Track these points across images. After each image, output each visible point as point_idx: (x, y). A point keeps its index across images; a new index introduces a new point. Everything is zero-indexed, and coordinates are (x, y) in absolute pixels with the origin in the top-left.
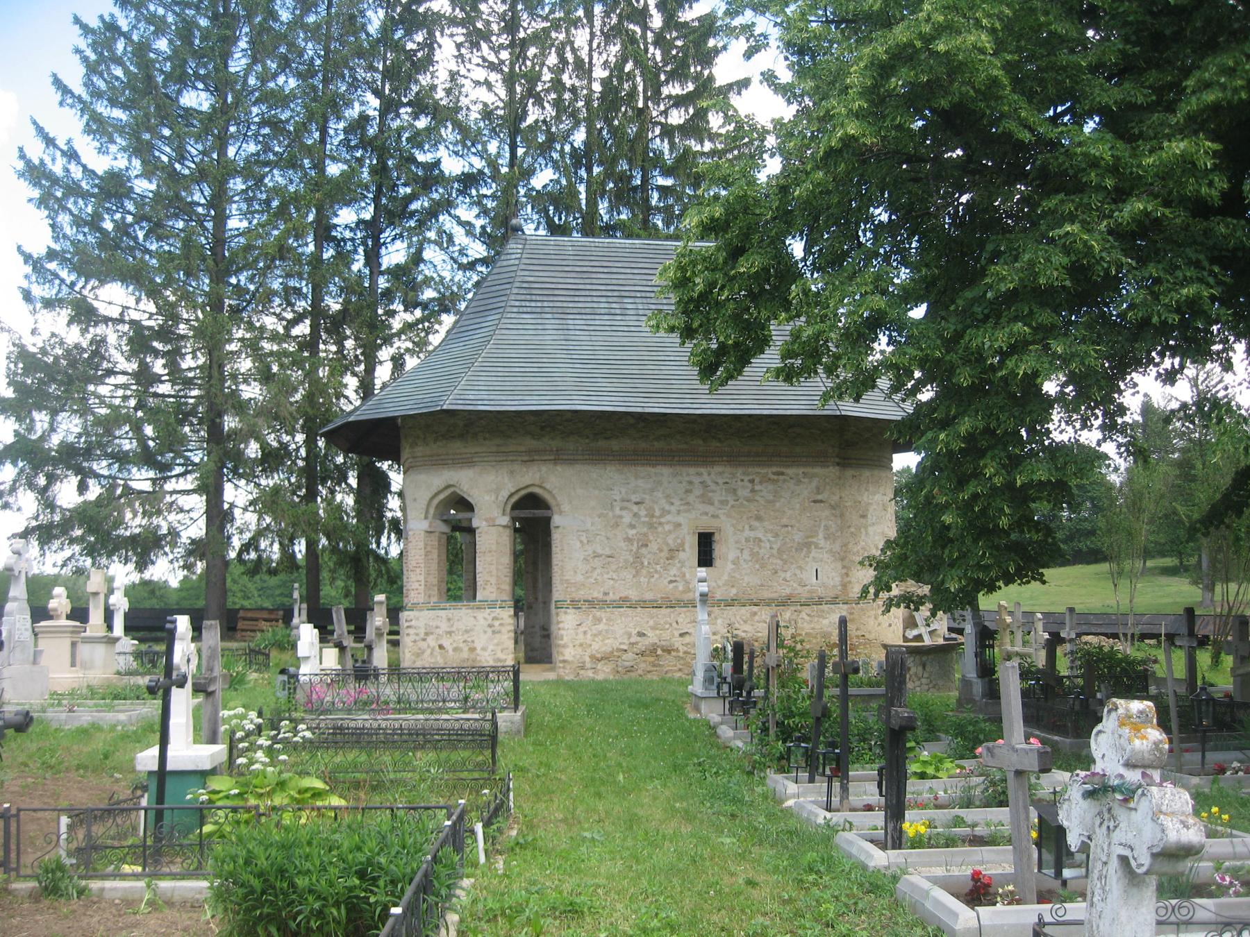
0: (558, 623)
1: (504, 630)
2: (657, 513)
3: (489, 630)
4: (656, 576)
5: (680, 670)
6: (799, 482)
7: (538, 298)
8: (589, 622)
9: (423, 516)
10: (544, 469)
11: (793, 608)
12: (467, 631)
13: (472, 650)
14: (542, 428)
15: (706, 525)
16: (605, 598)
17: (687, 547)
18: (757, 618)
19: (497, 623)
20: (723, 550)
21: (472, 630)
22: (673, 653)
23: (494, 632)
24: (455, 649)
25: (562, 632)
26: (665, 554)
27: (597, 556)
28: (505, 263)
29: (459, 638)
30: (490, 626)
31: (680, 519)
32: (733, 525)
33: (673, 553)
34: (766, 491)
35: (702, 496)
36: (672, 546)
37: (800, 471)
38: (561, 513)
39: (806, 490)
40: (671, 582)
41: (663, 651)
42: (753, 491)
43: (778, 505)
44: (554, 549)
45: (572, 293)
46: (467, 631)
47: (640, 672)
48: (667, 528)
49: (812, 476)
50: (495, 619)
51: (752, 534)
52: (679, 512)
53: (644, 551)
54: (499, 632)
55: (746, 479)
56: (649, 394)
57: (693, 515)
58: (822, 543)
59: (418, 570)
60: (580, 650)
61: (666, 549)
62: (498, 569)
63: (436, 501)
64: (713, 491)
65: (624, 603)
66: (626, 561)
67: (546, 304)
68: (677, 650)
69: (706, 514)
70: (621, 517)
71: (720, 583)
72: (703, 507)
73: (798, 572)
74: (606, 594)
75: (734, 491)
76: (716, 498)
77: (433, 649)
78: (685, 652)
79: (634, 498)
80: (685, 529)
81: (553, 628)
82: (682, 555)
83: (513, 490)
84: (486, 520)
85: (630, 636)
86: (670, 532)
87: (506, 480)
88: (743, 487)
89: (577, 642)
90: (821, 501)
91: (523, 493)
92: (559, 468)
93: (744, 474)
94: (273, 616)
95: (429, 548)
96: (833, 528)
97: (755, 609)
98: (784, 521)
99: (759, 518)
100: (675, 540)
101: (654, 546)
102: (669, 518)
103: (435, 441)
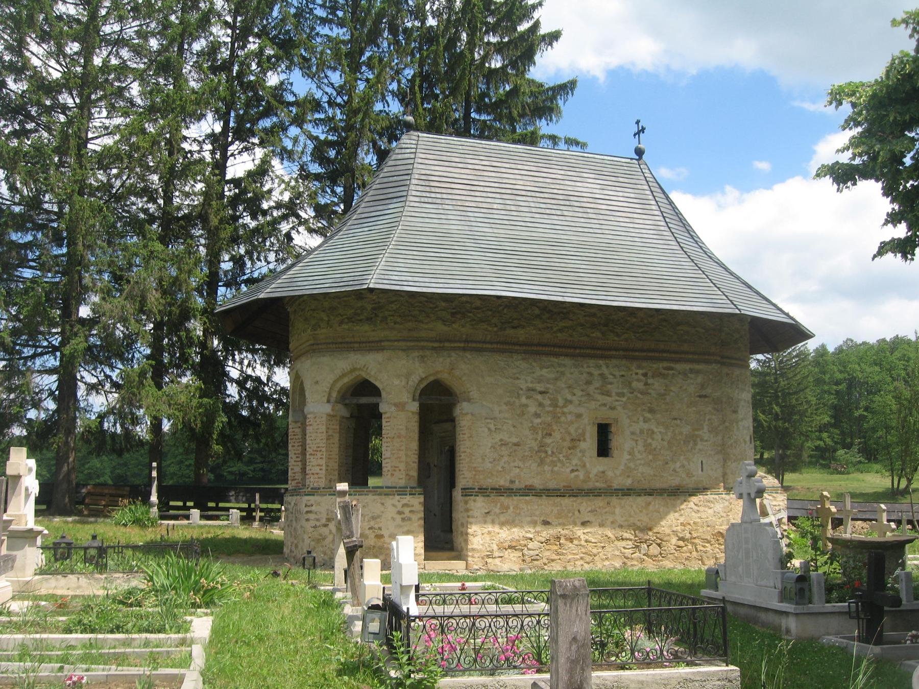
1: (414, 517)
2: (561, 402)
3: (398, 518)
4: (559, 465)
5: (582, 558)
7: (437, 190)
8: (497, 511)
9: (325, 399)
12: (374, 518)
15: (604, 416)
16: (511, 486)
17: (588, 435)
18: (651, 507)
19: (406, 510)
20: (620, 442)
21: (379, 517)
22: (575, 542)
23: (403, 519)
26: (567, 444)
30: (400, 513)
31: (581, 410)
32: (628, 417)
33: (575, 441)
34: (657, 384)
36: (574, 435)
37: (687, 366)
41: (566, 539)
42: (646, 384)
43: (668, 397)
45: (468, 187)
46: (374, 518)
47: (545, 561)
48: (569, 417)
49: (698, 372)
50: (404, 506)
51: (646, 426)
53: (548, 440)
54: (410, 519)
55: (640, 372)
56: (563, 284)
57: (593, 405)
59: (319, 454)
61: (568, 438)
62: (407, 455)
63: (339, 385)
64: (611, 383)
65: (529, 491)
69: (605, 405)
70: (526, 406)
71: (618, 472)
73: (685, 463)
74: (512, 482)
76: (614, 389)
79: (539, 387)
82: (583, 445)
84: (396, 405)
86: (572, 422)
87: (417, 364)
88: (638, 380)
90: (705, 396)
91: (432, 379)
92: (468, 355)
93: (639, 367)
94: (120, 492)
95: (330, 432)
97: (649, 498)
99: (651, 411)
100: (576, 430)
101: (557, 435)
102: (570, 408)
103: (341, 323)
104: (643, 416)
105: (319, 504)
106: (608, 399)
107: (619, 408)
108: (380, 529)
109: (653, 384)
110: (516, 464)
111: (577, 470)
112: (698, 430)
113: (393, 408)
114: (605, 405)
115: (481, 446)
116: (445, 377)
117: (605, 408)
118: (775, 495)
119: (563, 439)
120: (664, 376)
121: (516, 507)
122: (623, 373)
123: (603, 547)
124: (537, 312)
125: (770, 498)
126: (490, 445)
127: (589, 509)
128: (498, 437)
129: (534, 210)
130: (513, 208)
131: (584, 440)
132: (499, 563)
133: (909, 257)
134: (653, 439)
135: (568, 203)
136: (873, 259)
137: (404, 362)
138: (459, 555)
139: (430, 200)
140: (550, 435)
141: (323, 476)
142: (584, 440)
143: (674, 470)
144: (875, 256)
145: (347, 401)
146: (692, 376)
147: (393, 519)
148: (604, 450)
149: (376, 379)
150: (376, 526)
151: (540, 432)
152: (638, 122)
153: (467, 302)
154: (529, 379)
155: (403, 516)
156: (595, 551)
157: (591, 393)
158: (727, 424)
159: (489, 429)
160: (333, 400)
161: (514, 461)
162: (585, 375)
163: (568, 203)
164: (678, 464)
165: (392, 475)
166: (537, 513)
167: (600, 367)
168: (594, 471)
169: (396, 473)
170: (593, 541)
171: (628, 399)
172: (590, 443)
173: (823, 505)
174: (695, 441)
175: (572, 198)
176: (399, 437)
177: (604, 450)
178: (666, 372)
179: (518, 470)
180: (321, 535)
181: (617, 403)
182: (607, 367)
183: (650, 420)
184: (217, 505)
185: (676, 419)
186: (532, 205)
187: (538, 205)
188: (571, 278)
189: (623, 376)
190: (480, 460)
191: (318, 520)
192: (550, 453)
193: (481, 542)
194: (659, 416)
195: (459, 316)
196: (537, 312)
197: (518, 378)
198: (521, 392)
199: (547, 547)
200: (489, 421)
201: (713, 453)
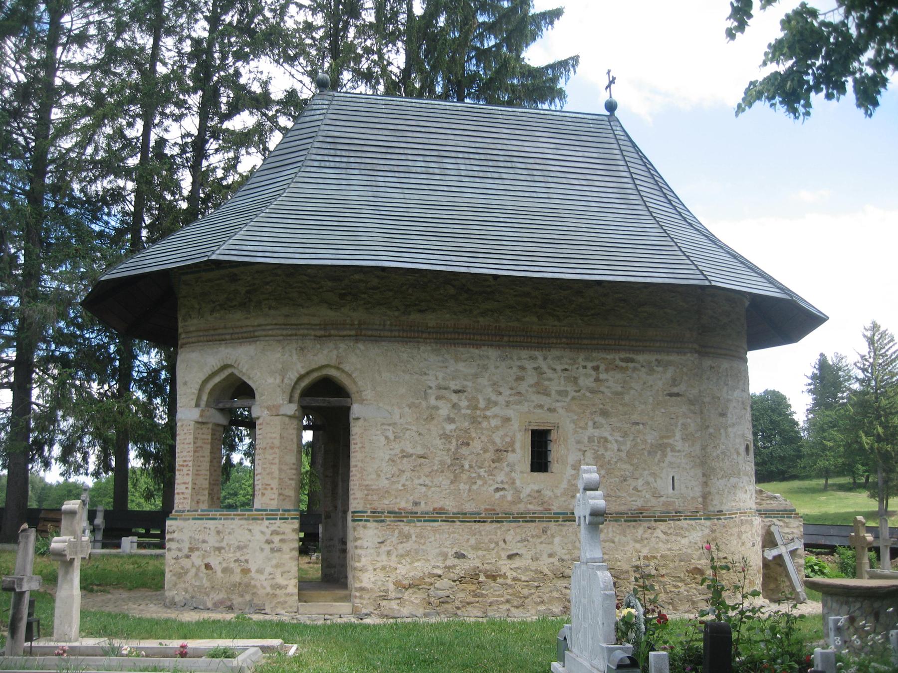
0: (356, 539)
1: (286, 547)
2: (482, 404)
4: (479, 482)
5: (508, 601)
6: (651, 371)
7: (344, 153)
8: (394, 540)
9: (193, 403)
10: (342, 346)
11: (646, 524)
12: (240, 548)
13: (246, 571)
14: (342, 296)
15: (541, 420)
16: (415, 509)
17: (518, 445)
19: (276, 539)
21: (246, 547)
22: (499, 580)
23: (272, 550)
24: (225, 570)
25: (359, 551)
26: (490, 455)
27: (406, 455)
28: (308, 119)
29: (230, 556)
30: (268, 542)
31: (510, 413)
32: (573, 421)
33: (500, 453)
34: (612, 381)
35: (537, 384)
37: (652, 357)
38: (362, 401)
39: (660, 380)
40: (497, 490)
41: (487, 577)
42: (597, 380)
43: (627, 398)
44: (352, 447)
46: (240, 548)
47: (457, 603)
48: (494, 422)
50: (274, 533)
51: (597, 433)
52: (508, 404)
53: (464, 451)
54: (279, 550)
55: (590, 365)
56: (474, 254)
57: (525, 408)
58: (679, 445)
59: (185, 469)
60: (381, 575)
61: (492, 449)
62: (280, 470)
63: (210, 385)
64: (550, 380)
65: (439, 515)
66: (442, 463)
67: (352, 160)
68: (504, 576)
69: (541, 406)
70: (437, 408)
71: (558, 492)
72: (537, 399)
73: (651, 479)
74: (416, 504)
75: (576, 379)
76: (554, 387)
77: (198, 569)
78: (514, 579)
79: (453, 385)
80: (515, 425)
81: (350, 545)
82: (511, 457)
83: (303, 372)
84: (268, 408)
85: (445, 556)
86: (497, 428)
87: (295, 357)
89: (379, 565)
90: (678, 395)
91: (315, 375)
92: (361, 346)
93: (587, 359)
95: (199, 443)
96: (692, 427)
98: (635, 417)
99: (604, 413)
101: (477, 446)
102: (495, 410)
103: (212, 312)
104: (592, 419)
105: (181, 530)
106: (545, 401)
107: (560, 411)
108: (247, 561)
109: (607, 380)
110: (421, 481)
111: (503, 489)
112: (668, 437)
113: (266, 412)
115: (376, 460)
116: (333, 372)
117: (540, 411)
118: (787, 520)
121: (420, 536)
122: (567, 367)
123: (537, 587)
124: (452, 291)
125: (781, 523)
126: (387, 457)
127: (518, 538)
128: (397, 447)
129: (463, 173)
130: (437, 171)
131: (513, 451)
132: (396, 607)
133: (801, 110)
134: (606, 449)
135: (509, 165)
136: (737, 115)
137: (279, 355)
138: (302, 598)
139: (332, 165)
140: (468, 444)
141: (189, 496)
142: (513, 451)
143: (635, 489)
144: (740, 109)
145: (221, 406)
146: (660, 369)
147: (262, 550)
148: (540, 461)
149: (249, 378)
150: (242, 558)
151: (454, 441)
152: (609, 72)
153: (360, 281)
154: (440, 375)
155: (272, 546)
156: (526, 592)
157: (523, 392)
158: (711, 430)
159: (387, 438)
160: (203, 403)
161: (419, 478)
162: (515, 369)
163: (509, 165)
165: (263, 494)
166: (447, 543)
168: (527, 491)
169: (268, 492)
170: (524, 578)
172: (522, 455)
173: (857, 533)
175: (515, 159)
176: (272, 448)
177: (540, 461)
178: (624, 364)
179: (424, 489)
180: (182, 568)
181: (558, 404)
182: (545, 359)
183: (602, 426)
184: (148, 531)
185: (638, 424)
186: (463, 167)
187: (469, 167)
188: (490, 246)
189: (566, 370)
190: (374, 476)
191: (180, 550)
192: (467, 467)
193: (373, 579)
194: (613, 420)
195: (349, 298)
196: (452, 291)
197: (425, 374)
198: (430, 391)
199: (462, 586)
200: (387, 427)
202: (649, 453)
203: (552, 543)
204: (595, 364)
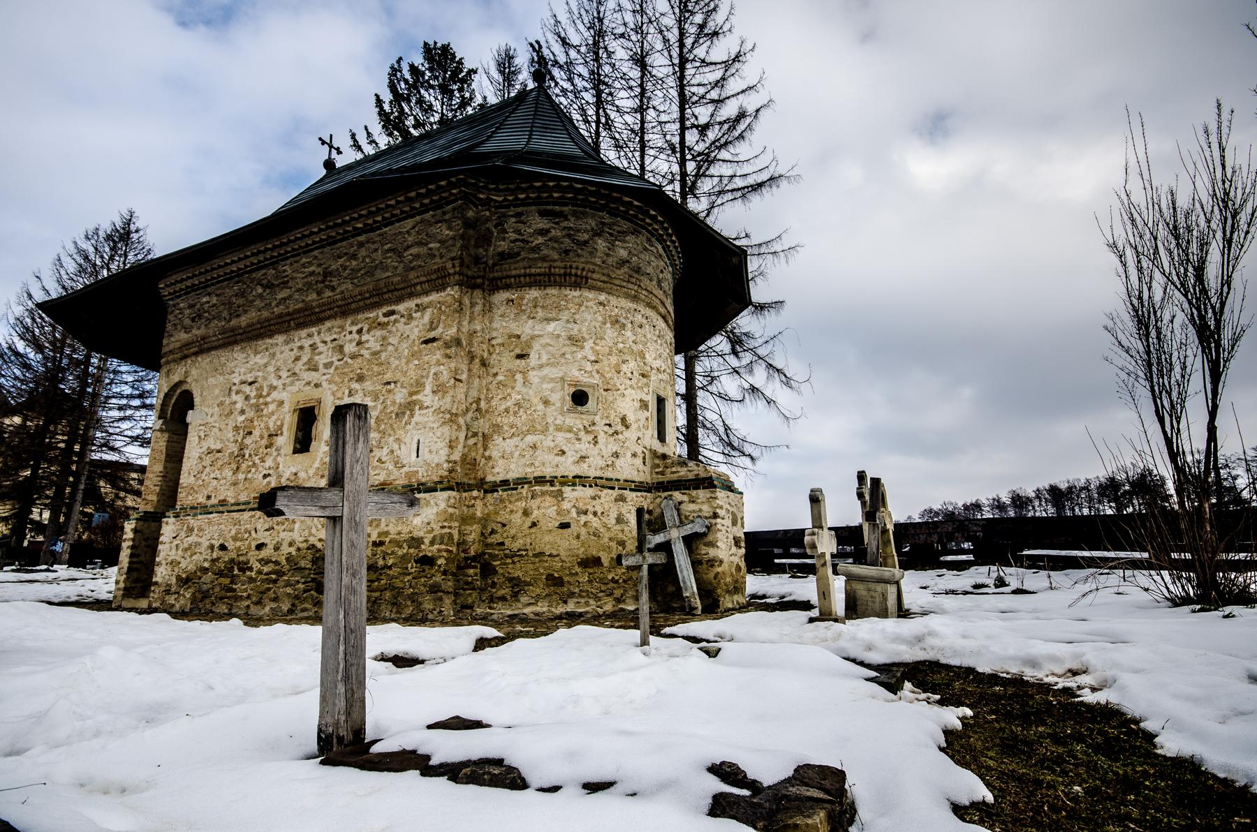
32: (333, 394)
34: (372, 340)
37: (411, 304)
40: (265, 476)
41: (240, 570)
42: (359, 343)
43: (383, 355)
53: (248, 441)
55: (355, 329)
68: (251, 569)
69: (308, 383)
70: (235, 403)
71: (311, 472)
73: (396, 446)
76: (321, 360)
89: (170, 559)
90: (434, 340)
93: (353, 323)
98: (388, 377)
101: (256, 433)
102: (275, 395)
109: (367, 341)
110: (212, 475)
114: (308, 383)
118: (694, 493)
119: (262, 437)
120: (382, 325)
122: (335, 336)
143: (380, 460)
158: (500, 378)
164: (385, 451)
167: (310, 335)
171: (336, 368)
174: (412, 410)
185: (389, 383)
201: (435, 425)
202: (397, 415)
203: (292, 530)
204: (359, 326)
